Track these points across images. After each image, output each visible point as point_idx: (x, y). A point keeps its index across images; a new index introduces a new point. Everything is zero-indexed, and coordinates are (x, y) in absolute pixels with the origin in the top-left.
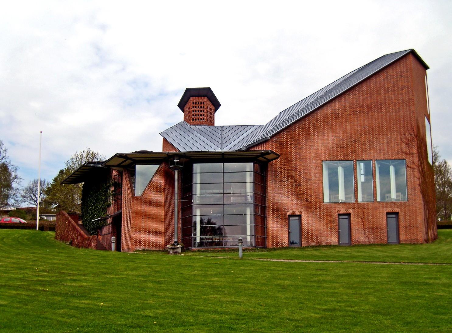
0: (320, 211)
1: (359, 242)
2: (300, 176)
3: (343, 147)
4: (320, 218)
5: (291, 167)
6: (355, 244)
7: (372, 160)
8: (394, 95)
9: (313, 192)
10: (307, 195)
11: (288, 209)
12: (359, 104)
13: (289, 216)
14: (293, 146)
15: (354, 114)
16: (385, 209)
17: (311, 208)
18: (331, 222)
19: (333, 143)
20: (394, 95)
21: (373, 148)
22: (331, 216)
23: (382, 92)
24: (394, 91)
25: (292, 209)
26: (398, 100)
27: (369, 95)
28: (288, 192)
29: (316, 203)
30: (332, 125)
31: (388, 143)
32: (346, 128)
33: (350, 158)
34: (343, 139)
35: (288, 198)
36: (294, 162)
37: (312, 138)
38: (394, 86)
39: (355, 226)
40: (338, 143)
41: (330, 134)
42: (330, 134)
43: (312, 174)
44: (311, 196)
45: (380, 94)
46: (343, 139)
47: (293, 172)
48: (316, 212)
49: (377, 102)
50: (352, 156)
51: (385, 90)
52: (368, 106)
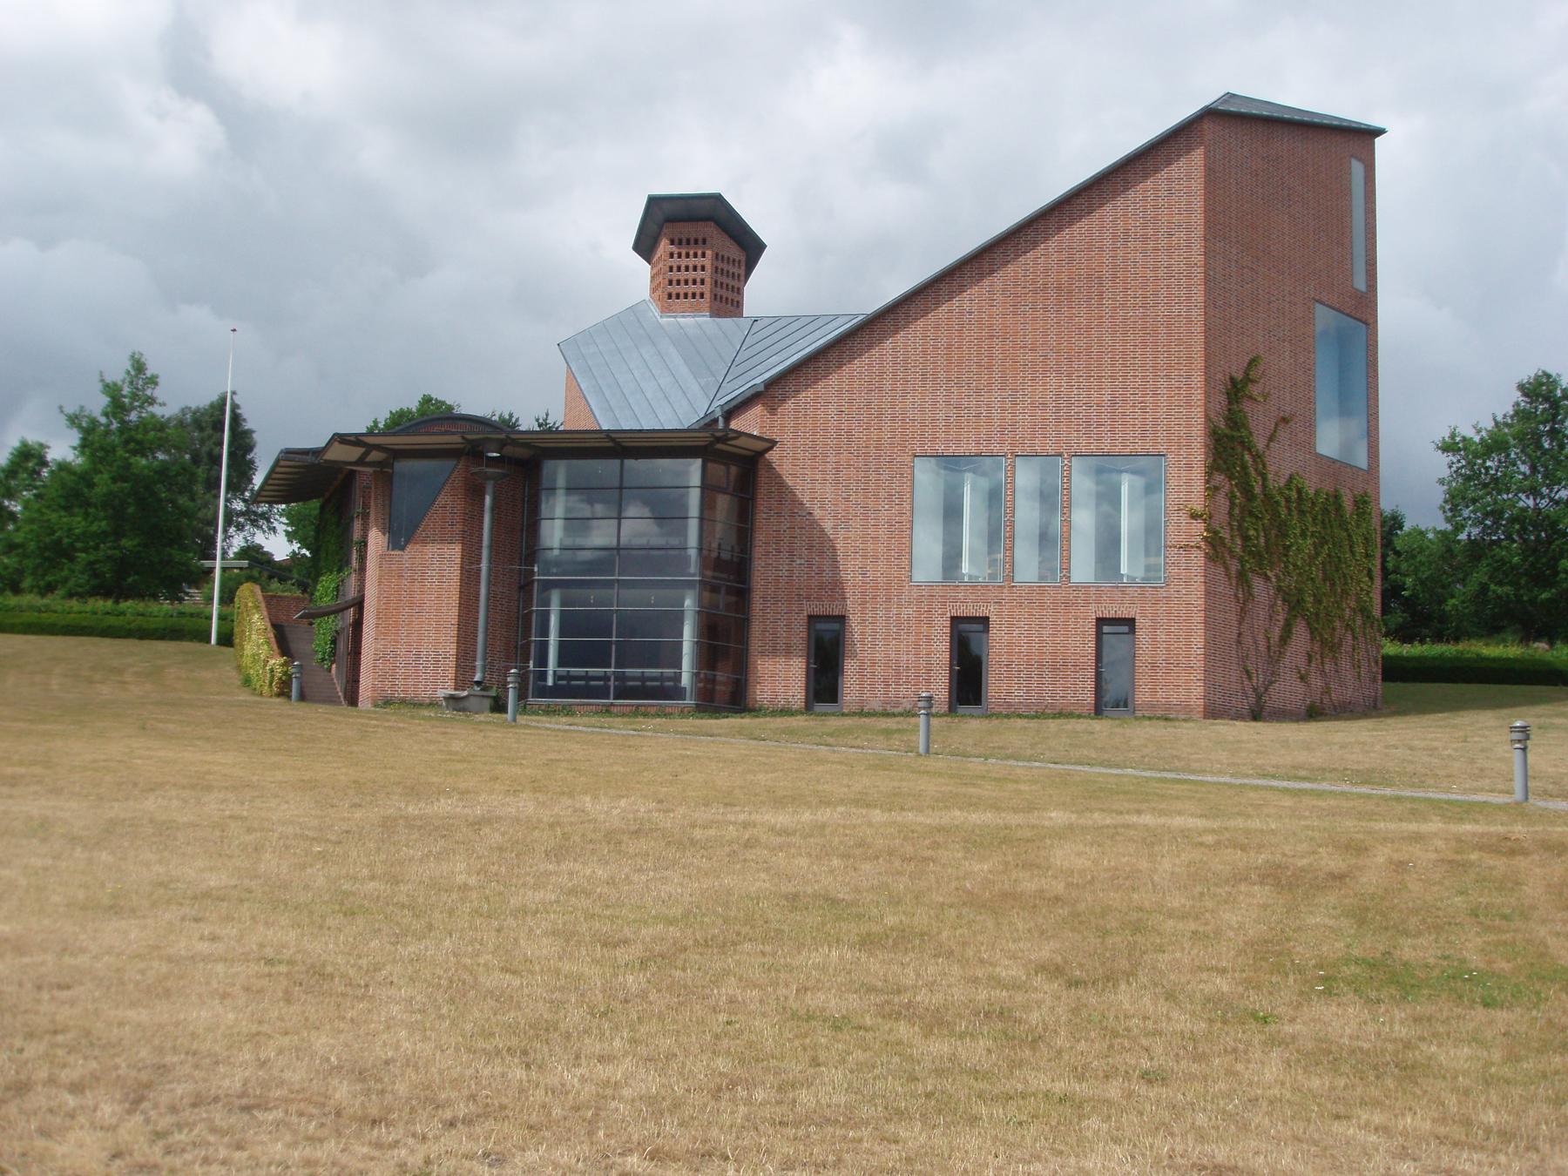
0: (900, 605)
1: (1010, 705)
2: (847, 499)
3: (978, 416)
4: (898, 626)
5: (824, 472)
6: (997, 709)
7: (1060, 455)
8: (1145, 251)
9: (881, 548)
10: (864, 557)
11: (808, 598)
12: (1034, 282)
13: (810, 617)
14: (832, 409)
15: (1015, 313)
16: (1092, 607)
17: (874, 597)
18: (929, 639)
19: (948, 403)
20: (1145, 251)
21: (1069, 419)
22: (930, 624)
23: (1108, 243)
24: (1145, 238)
25: (819, 599)
26: (1156, 269)
27: (1065, 255)
28: (810, 548)
29: (889, 583)
30: (949, 346)
31: (1113, 403)
32: (990, 357)
33: (995, 448)
34: (978, 391)
35: (810, 566)
36: (832, 459)
37: (887, 385)
38: (1145, 226)
39: (1000, 654)
40: (965, 402)
41: (942, 375)
42: (942, 375)
43: (882, 494)
44: (876, 559)
45: (1101, 249)
46: (978, 391)
47: (829, 488)
48: (888, 610)
49: (1089, 276)
50: (1002, 442)
51: (1115, 236)
52: (1059, 288)
